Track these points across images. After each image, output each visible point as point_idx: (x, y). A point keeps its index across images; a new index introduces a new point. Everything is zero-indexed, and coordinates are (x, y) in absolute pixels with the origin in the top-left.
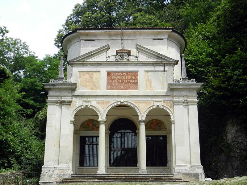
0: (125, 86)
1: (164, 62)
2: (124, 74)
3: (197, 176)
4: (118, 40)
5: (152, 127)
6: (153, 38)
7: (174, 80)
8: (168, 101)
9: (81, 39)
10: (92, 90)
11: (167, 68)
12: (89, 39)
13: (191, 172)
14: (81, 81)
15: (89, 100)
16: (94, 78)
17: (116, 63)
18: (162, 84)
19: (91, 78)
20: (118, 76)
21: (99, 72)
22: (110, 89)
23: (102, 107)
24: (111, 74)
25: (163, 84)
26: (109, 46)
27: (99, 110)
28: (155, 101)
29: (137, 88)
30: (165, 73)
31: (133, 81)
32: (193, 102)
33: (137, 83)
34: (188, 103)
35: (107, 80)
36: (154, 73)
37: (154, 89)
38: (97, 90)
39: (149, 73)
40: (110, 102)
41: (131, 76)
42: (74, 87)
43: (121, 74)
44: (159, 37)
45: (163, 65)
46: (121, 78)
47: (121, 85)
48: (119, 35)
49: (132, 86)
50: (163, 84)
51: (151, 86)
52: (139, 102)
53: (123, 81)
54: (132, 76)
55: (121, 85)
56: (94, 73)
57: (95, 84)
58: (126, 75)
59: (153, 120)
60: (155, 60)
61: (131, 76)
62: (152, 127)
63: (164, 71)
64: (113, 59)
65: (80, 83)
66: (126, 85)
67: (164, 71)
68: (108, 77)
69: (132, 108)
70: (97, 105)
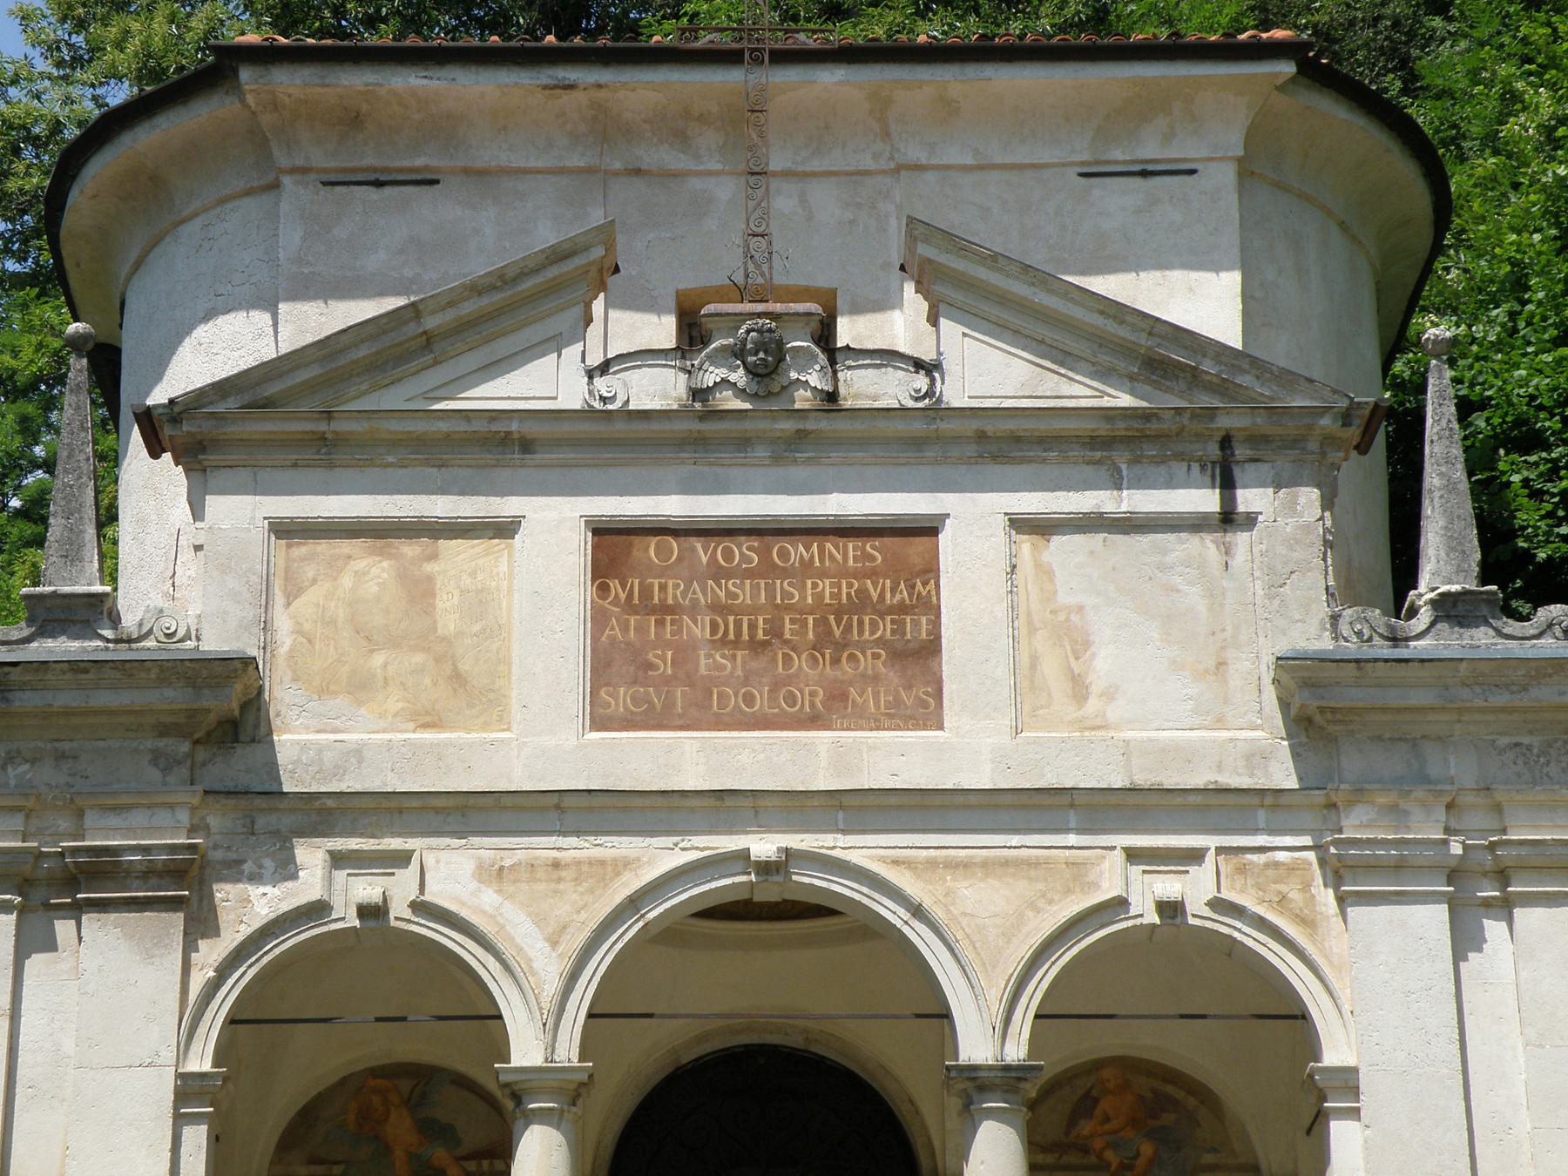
0: (789, 681)
1: (1224, 422)
2: (783, 554)
4: (696, 183)
5: (1085, 1151)
6: (1081, 151)
7: (1335, 618)
8: (1282, 856)
9: (284, 162)
10: (426, 726)
11: (1249, 498)
12: (370, 160)
14: (298, 631)
15: (395, 843)
16: (447, 603)
18: (1212, 663)
19: (420, 593)
20: (719, 574)
21: (505, 529)
22: (629, 724)
23: (539, 920)
24: (637, 553)
25: (1221, 664)
26: (610, 246)
27: (508, 956)
28: (1133, 855)
29: (928, 713)
30: (1241, 539)
31: (886, 628)
33: (931, 648)
34: (1502, 876)
35: (599, 619)
36: (1119, 539)
37: (1114, 713)
38: (485, 727)
39: (1057, 540)
40: (625, 864)
41: (856, 574)
42: (229, 702)
43: (745, 551)
44: (1150, 149)
45: (1214, 451)
46: (744, 593)
47: (746, 681)
48: (702, 119)
49: (876, 678)
50: (1221, 664)
51: (1079, 689)
52: (952, 865)
53: (775, 631)
54: (873, 574)
55: (746, 681)
56: (443, 544)
57: (464, 666)
58: (807, 565)
59: (1097, 1065)
60: (1125, 400)
61: (856, 574)
62: (1085, 1151)
63: (1228, 519)
65: (291, 655)
66: (810, 675)
68: (603, 589)
69: (875, 931)
70: (489, 898)
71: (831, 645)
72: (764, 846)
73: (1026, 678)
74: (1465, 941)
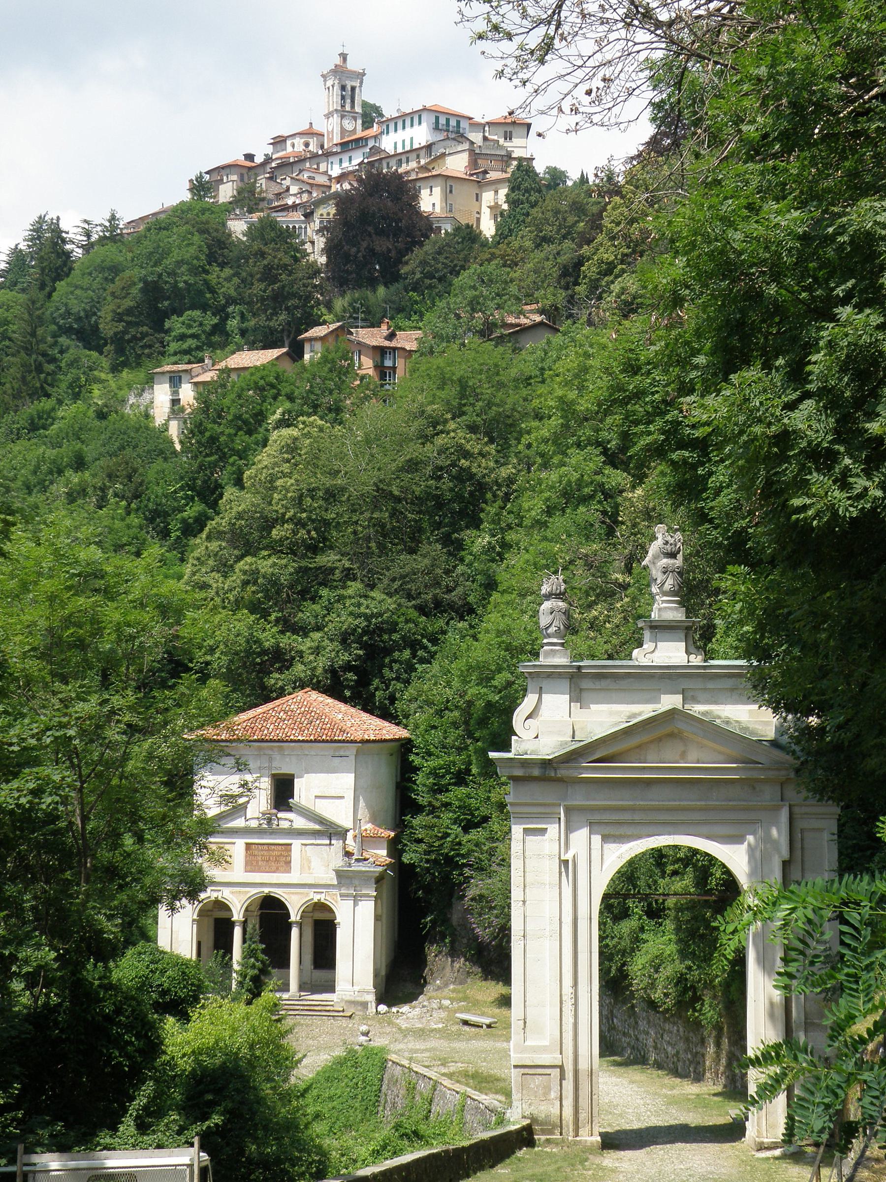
3: (364, 1005)
13: (359, 999)
17: (258, 832)
29: (289, 871)
32: (368, 896)
43: (266, 847)
44: (342, 753)
60: (317, 827)
63: (330, 844)
64: (254, 824)
67: (330, 844)
71: (277, 861)
72: (266, 890)
73: (302, 868)
74: (355, 905)
